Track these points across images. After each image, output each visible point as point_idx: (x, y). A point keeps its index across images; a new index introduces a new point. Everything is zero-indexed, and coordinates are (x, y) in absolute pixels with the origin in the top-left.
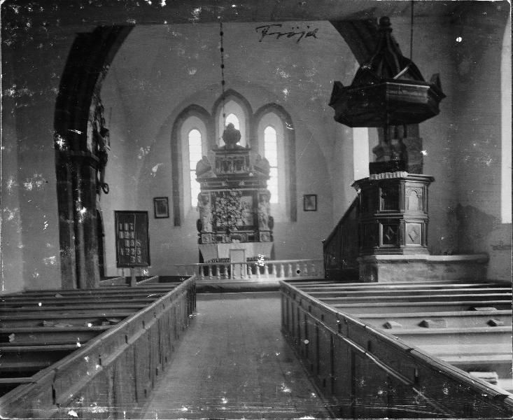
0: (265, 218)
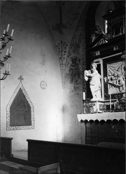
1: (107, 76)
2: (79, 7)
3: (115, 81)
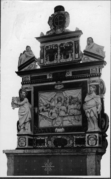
1: (38, 107)
3: (47, 113)
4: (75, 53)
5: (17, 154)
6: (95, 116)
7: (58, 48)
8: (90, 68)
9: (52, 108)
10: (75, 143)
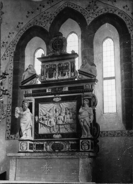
0: (85, 124)
1: (38, 116)
2: (9, 37)
3: (46, 122)
4: (71, 72)
5: (19, 156)
6: (88, 124)
7: (56, 67)
8: (84, 84)
9: (49, 117)
10: (70, 147)
